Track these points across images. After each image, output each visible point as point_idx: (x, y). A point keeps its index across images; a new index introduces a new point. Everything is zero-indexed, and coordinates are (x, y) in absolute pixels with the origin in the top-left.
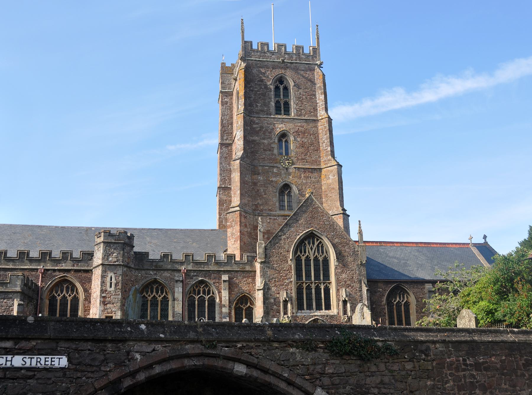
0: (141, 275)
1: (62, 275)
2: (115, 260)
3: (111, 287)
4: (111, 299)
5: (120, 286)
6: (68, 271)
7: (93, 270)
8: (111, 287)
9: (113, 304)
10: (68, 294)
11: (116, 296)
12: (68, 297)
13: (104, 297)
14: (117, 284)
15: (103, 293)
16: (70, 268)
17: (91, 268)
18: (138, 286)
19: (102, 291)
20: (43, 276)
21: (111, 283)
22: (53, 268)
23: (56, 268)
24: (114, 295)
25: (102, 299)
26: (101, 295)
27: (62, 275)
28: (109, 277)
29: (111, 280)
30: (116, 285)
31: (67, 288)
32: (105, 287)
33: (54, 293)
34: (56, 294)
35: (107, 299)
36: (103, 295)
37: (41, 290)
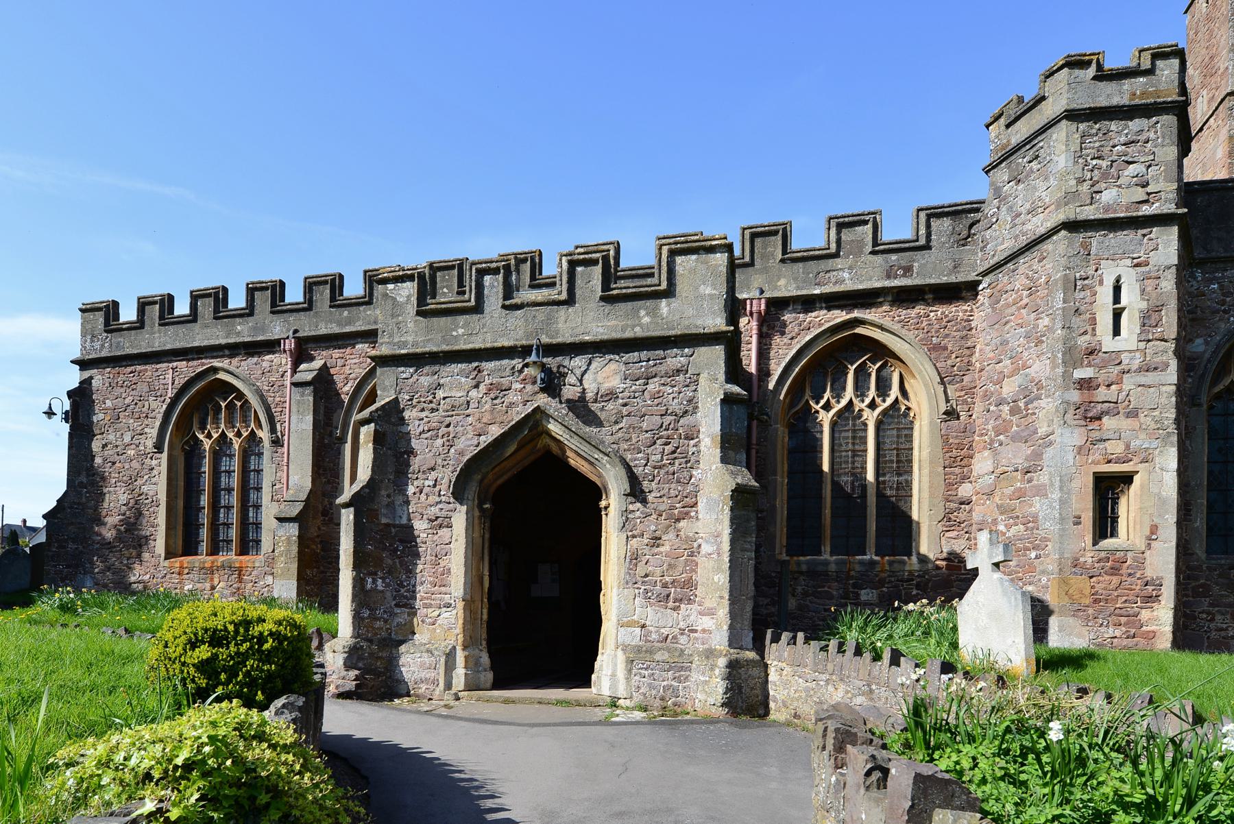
0: (1221, 287)
1: (839, 316)
2: (1140, 194)
3: (1117, 331)
4: (1120, 391)
5: (1169, 323)
6: (867, 298)
7: (979, 282)
8: (1117, 331)
9: (1133, 414)
10: (867, 401)
11: (1150, 378)
12: (867, 413)
13: (1086, 385)
14: (1155, 316)
15: (1077, 364)
16: (878, 285)
17: (972, 277)
18: (1207, 343)
19: (1073, 357)
20: (765, 329)
21: (1117, 315)
22: (804, 292)
23: (817, 292)
24: (1140, 370)
25: (1075, 396)
26: (1066, 375)
27: (839, 316)
28: (1109, 282)
29: (1117, 298)
30: (1148, 319)
31: (861, 373)
32: (1085, 333)
33: (807, 397)
34: (817, 403)
35: (1102, 393)
36: (1079, 374)
37: (759, 387)
